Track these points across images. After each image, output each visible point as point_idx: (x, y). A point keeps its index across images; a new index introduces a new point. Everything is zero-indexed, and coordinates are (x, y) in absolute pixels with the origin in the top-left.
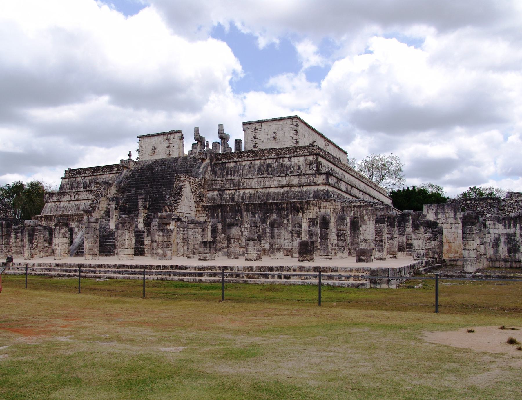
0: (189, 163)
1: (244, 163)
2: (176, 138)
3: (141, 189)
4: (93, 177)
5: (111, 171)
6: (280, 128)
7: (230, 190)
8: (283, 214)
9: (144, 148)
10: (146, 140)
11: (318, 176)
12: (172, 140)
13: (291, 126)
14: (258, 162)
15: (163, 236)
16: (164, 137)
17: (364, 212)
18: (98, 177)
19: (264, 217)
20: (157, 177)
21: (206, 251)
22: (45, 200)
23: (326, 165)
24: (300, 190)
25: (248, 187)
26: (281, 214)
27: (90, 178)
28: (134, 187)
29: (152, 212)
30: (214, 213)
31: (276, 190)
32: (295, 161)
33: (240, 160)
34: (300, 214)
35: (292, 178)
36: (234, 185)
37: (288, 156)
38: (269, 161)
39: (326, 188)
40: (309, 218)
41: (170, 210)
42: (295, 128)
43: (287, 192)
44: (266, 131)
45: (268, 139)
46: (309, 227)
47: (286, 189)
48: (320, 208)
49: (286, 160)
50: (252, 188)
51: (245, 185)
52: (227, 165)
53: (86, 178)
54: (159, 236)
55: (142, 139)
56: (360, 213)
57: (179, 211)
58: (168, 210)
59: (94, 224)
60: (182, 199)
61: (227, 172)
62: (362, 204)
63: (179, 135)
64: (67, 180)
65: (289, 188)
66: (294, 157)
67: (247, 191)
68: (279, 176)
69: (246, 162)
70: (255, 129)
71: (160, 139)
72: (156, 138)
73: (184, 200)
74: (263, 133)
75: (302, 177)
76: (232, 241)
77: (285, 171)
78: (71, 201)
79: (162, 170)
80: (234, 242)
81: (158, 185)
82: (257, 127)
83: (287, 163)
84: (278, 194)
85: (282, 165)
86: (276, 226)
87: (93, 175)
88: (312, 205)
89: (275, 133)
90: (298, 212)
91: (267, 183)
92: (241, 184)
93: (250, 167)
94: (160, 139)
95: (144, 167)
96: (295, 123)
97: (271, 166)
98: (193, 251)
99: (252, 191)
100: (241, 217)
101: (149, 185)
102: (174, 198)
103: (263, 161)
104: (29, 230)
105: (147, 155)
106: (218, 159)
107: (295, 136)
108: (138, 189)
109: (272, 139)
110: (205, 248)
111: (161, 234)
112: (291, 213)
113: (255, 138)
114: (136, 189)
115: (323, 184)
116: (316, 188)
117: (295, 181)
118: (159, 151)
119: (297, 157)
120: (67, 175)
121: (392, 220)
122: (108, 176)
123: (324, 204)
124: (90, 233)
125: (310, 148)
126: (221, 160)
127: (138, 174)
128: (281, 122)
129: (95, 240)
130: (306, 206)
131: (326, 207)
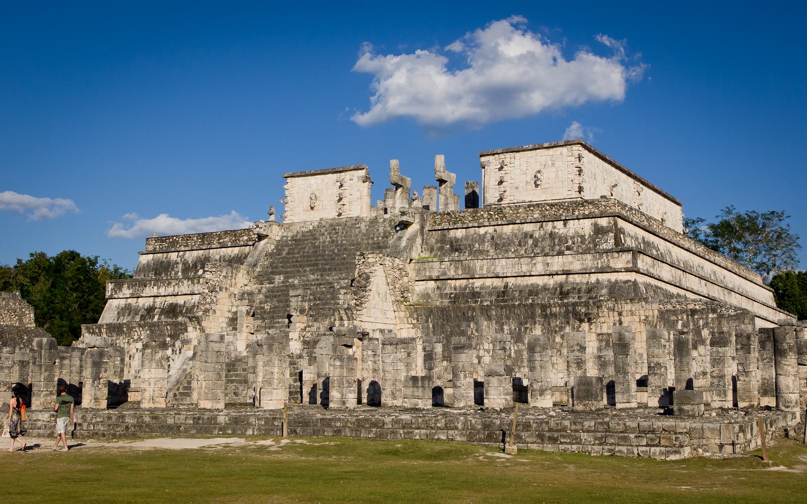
0: (381, 229)
1: (482, 231)
2: (355, 179)
3: (294, 277)
4: (201, 252)
6: (550, 163)
8: (552, 325)
9: (295, 196)
11: (616, 255)
14: (508, 229)
15: (341, 367)
17: (701, 322)
18: (211, 250)
19: (520, 330)
20: (322, 256)
21: (416, 394)
22: (108, 294)
23: (632, 234)
24: (585, 281)
25: (490, 275)
26: (549, 324)
27: (195, 253)
28: (279, 274)
29: (316, 320)
30: (427, 321)
31: (540, 281)
32: (574, 227)
33: (476, 225)
34: (585, 326)
35: (570, 258)
36: (464, 269)
37: (563, 218)
38: (528, 228)
39: (632, 276)
40: (599, 335)
41: (348, 317)
42: (577, 164)
43: (561, 286)
46: (600, 349)
48: (620, 314)
49: (560, 224)
51: (485, 272)
52: (452, 233)
54: (334, 365)
56: (694, 325)
57: (364, 318)
58: (345, 317)
59: (217, 345)
60: (370, 298)
61: (452, 246)
62: (697, 307)
64: (151, 256)
66: (573, 219)
67: (488, 282)
68: (546, 255)
73: (374, 299)
75: (589, 257)
76: (462, 375)
77: (558, 245)
78: (157, 296)
79: (333, 241)
80: (465, 377)
81: (325, 270)
84: (545, 288)
85: (551, 234)
86: (538, 349)
88: (606, 310)
89: (539, 172)
90: (581, 321)
91: (525, 269)
92: (478, 268)
93: (493, 238)
95: (299, 236)
96: (576, 154)
97: (531, 236)
98: (393, 393)
99: (498, 283)
100: (477, 331)
101: (308, 269)
104: (92, 355)
106: (435, 222)
107: (577, 177)
108: (288, 278)
110: (415, 389)
111: (338, 363)
112: (568, 323)
114: (284, 278)
115: (628, 270)
116: (613, 277)
117: (577, 266)
119: (579, 219)
121: (745, 341)
124: (209, 361)
125: (603, 203)
126: (439, 224)
127: (287, 249)
128: (551, 151)
129: (219, 374)
130: (595, 311)
131: (632, 313)
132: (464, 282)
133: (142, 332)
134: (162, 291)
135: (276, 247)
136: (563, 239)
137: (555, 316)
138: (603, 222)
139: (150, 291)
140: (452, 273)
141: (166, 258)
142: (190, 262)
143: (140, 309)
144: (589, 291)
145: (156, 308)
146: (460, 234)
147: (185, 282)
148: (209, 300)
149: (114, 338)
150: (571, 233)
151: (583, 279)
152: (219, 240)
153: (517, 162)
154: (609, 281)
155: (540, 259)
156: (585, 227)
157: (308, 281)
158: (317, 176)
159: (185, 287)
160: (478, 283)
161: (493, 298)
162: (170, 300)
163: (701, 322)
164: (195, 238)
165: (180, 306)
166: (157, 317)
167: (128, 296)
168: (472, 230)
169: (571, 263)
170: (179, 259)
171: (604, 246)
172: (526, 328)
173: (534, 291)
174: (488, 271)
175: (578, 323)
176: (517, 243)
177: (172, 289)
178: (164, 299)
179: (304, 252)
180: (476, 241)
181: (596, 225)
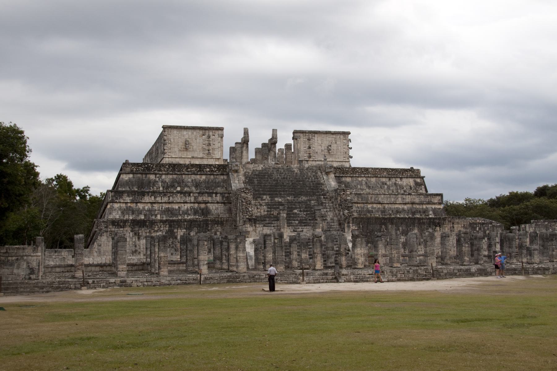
1: (360, 179)
2: (216, 135)
4: (175, 176)
5: (200, 171)
6: (334, 141)
7: (357, 203)
9: (172, 140)
10: (175, 132)
12: (212, 137)
13: (344, 141)
14: (373, 180)
16: (201, 132)
17: (486, 228)
18: (184, 176)
24: (421, 207)
27: (171, 176)
28: (264, 194)
31: (400, 207)
34: (438, 228)
35: (414, 197)
36: (362, 199)
44: (320, 142)
45: (322, 151)
47: (409, 206)
48: (453, 224)
50: (380, 203)
51: (373, 200)
52: (344, 179)
53: (163, 177)
55: (170, 130)
63: (220, 132)
64: (131, 176)
65: (411, 205)
67: (375, 206)
69: (362, 178)
70: (309, 140)
71: (195, 133)
72: (190, 132)
74: (316, 144)
75: (422, 196)
78: (155, 203)
79: (284, 178)
82: (311, 137)
83: (400, 183)
84: (403, 209)
87: (175, 174)
90: (436, 226)
91: (393, 200)
93: (366, 183)
94: (195, 133)
97: (386, 184)
102: (349, 210)
103: (377, 178)
105: (176, 150)
109: (326, 151)
111: (467, 245)
113: (310, 148)
114: (270, 197)
116: (433, 206)
117: (417, 200)
118: (195, 147)
119: (407, 178)
120: (128, 170)
122: (198, 177)
123: (457, 221)
128: (334, 136)
131: (458, 223)
132: (362, 205)
133: (162, 226)
134: (159, 199)
135: (246, 178)
136: (402, 187)
137: (424, 223)
138: (418, 180)
139: (147, 199)
140: (356, 200)
141: (146, 177)
142: (167, 181)
143: (141, 211)
144: (424, 212)
145: (155, 210)
146: (348, 180)
147: (179, 195)
148: (250, 209)
149: (137, 229)
150: (405, 184)
151: (421, 207)
152: (187, 169)
153: (316, 138)
154: (432, 208)
155: (400, 196)
156: (411, 182)
157: (288, 200)
158: (188, 130)
159: (178, 198)
160: (369, 206)
161: (380, 213)
162: (167, 206)
163: (486, 228)
164: (167, 167)
165: (176, 210)
166: (159, 217)
167: (129, 201)
168: (355, 179)
169: (414, 199)
170: (157, 179)
171: (421, 191)
172: (410, 229)
173: (398, 211)
174: (375, 200)
175: (434, 227)
176: (379, 186)
177: (168, 199)
178: (161, 205)
179: (269, 183)
180: (358, 184)
181: (415, 181)
